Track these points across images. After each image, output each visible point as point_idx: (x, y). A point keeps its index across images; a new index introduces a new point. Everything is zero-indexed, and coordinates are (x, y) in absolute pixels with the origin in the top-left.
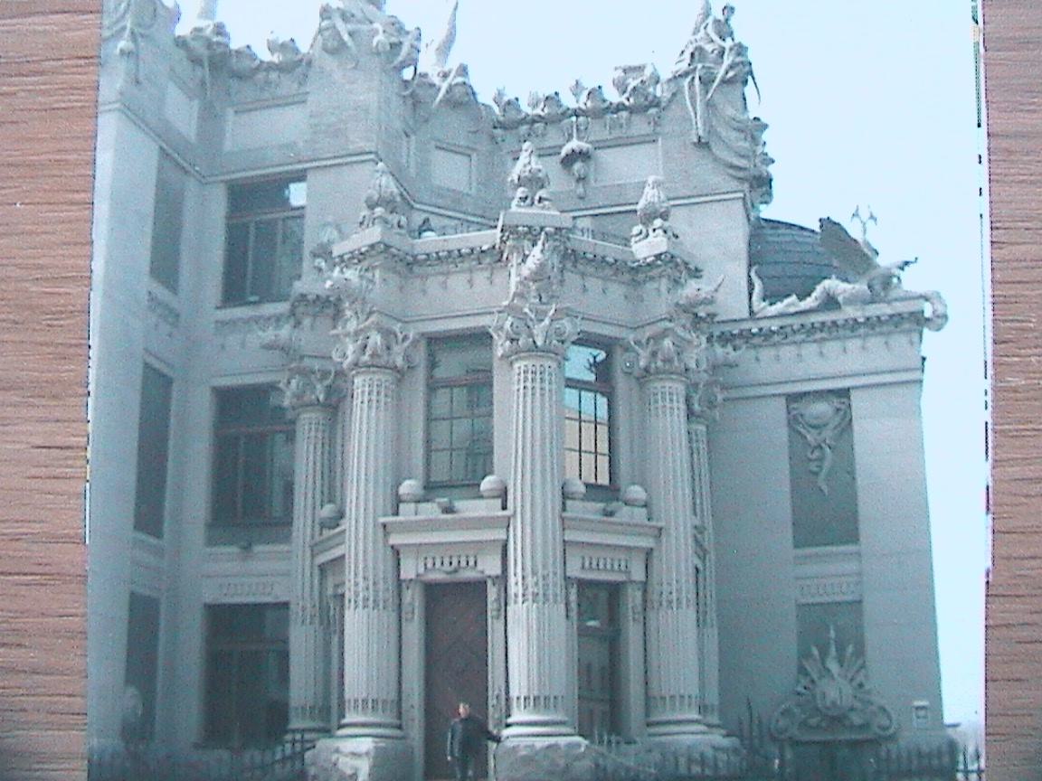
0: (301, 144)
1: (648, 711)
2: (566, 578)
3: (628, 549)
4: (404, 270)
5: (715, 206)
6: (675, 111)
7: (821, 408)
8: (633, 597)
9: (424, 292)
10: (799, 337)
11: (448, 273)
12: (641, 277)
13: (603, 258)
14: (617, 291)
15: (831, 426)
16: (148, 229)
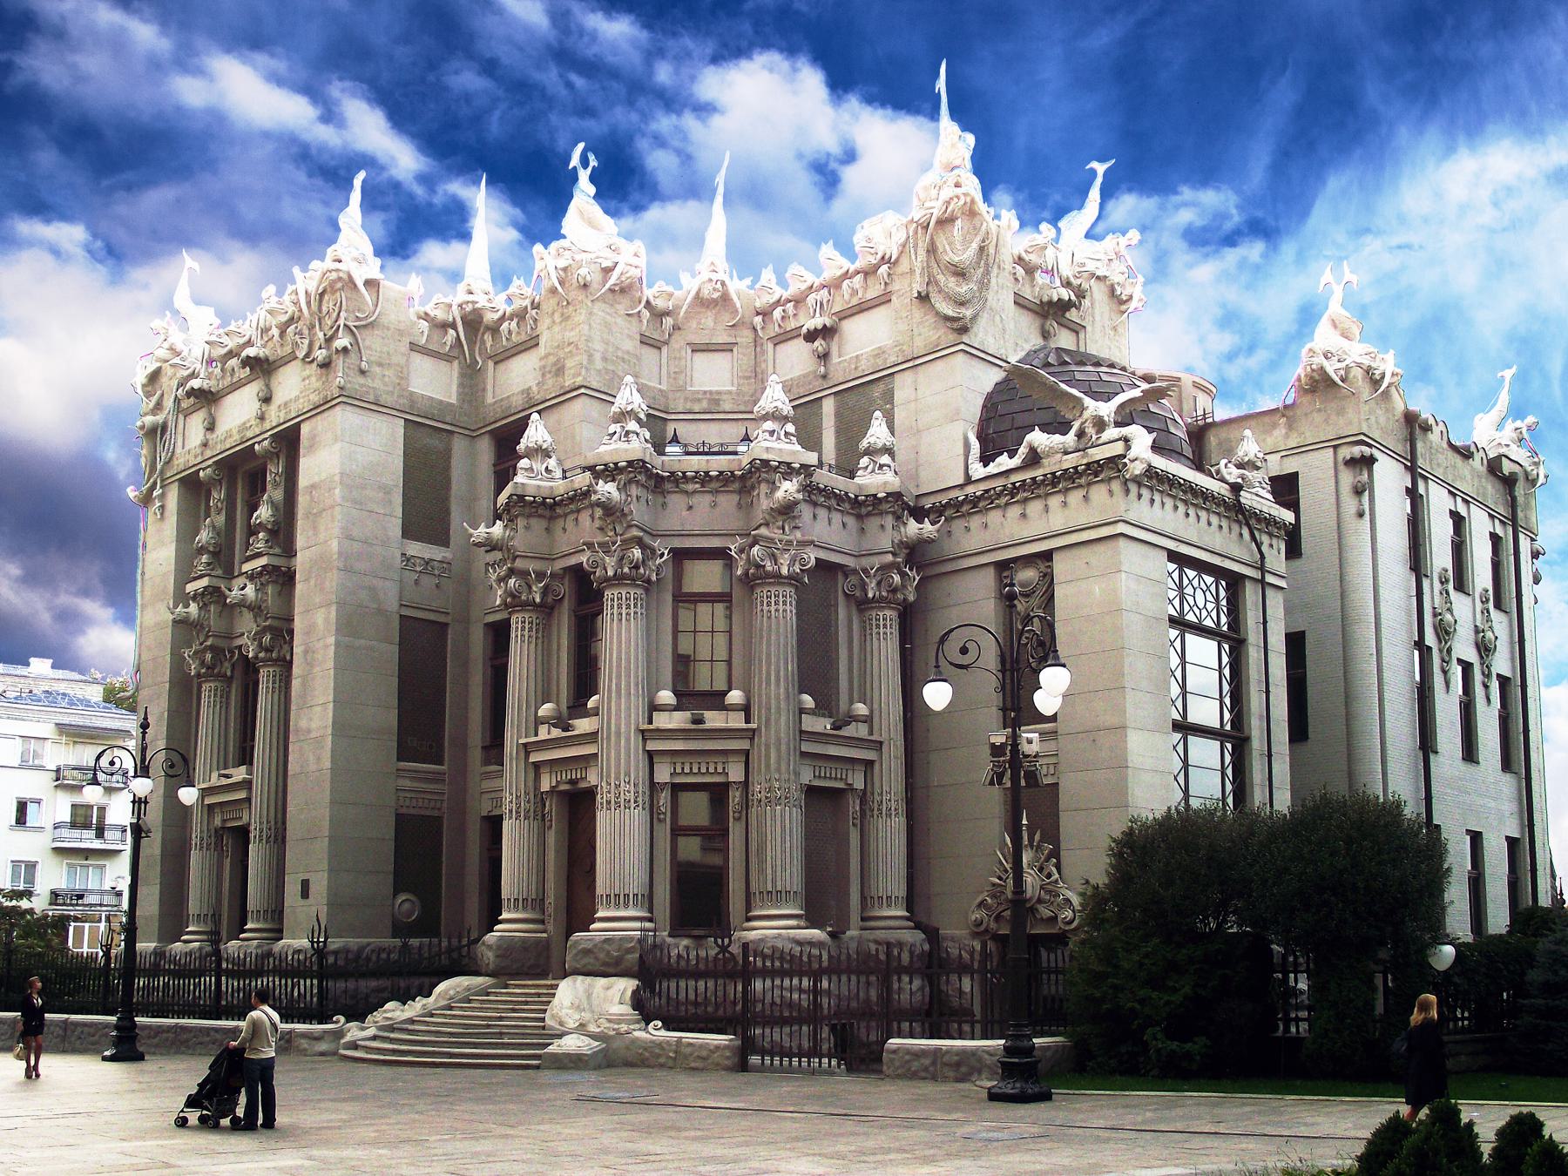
0: (535, 389)
1: (864, 906)
2: (653, 786)
3: (725, 753)
4: (547, 513)
5: (939, 362)
6: (904, 266)
7: (1028, 575)
8: (735, 797)
9: (564, 529)
10: (1003, 500)
11: (578, 511)
12: (749, 484)
13: (707, 473)
14: (728, 501)
15: (1039, 593)
16: (398, 500)
